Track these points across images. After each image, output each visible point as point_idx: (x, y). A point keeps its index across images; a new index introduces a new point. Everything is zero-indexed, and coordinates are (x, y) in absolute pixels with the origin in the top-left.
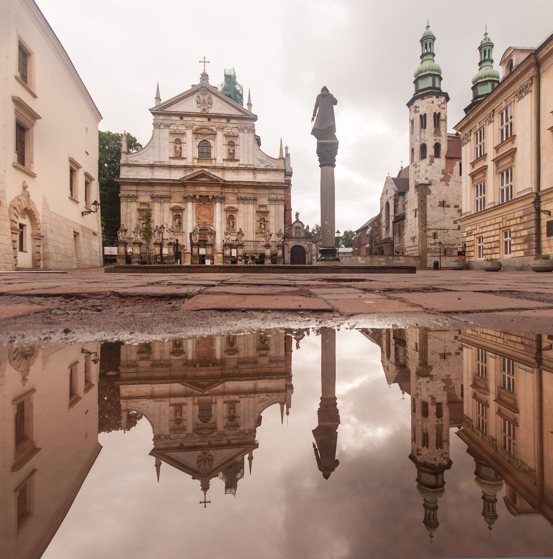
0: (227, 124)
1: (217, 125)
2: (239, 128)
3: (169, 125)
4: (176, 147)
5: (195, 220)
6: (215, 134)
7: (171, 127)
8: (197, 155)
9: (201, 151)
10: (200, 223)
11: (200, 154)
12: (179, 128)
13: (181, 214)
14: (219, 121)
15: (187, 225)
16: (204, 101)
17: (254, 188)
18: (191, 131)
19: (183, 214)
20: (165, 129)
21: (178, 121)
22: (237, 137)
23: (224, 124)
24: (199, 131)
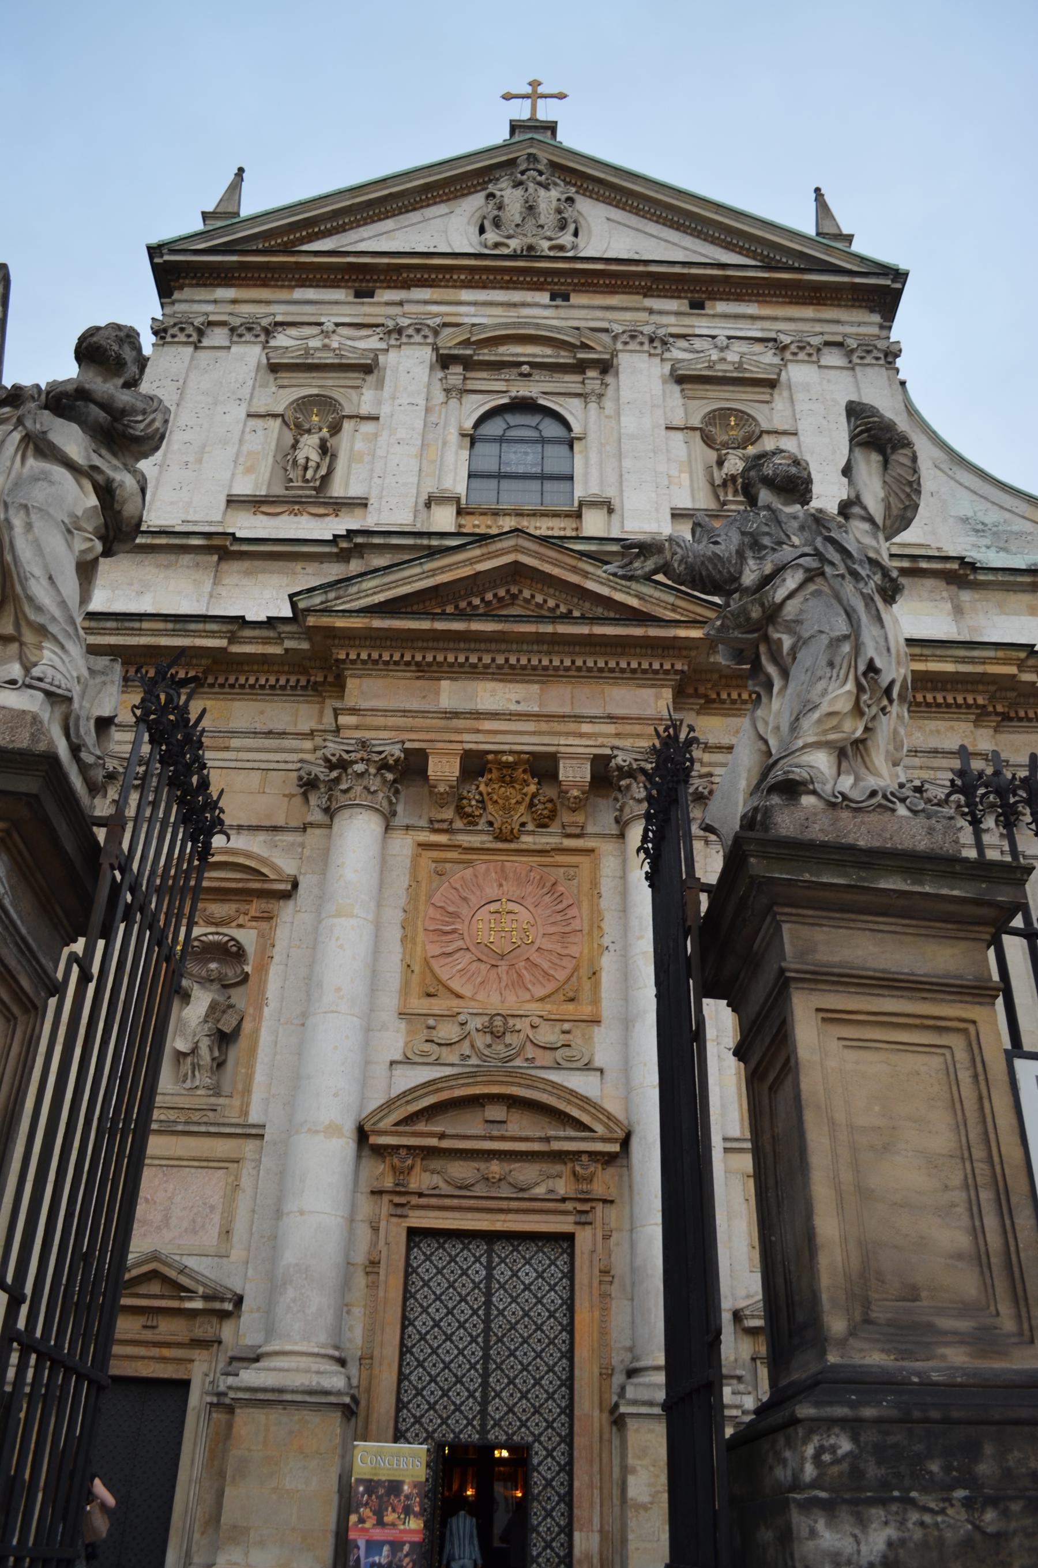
0: (687, 321)
1: (619, 321)
2: (786, 339)
3: (265, 322)
4: (294, 447)
5: (390, 1001)
6: (606, 367)
7: (281, 340)
8: (458, 484)
9: (492, 466)
10: (448, 1031)
11: (477, 483)
12: (335, 345)
13: (247, 937)
14: (638, 305)
15: (300, 1052)
16: (531, 209)
17: (981, 716)
18: (427, 354)
19: (267, 943)
20: (235, 349)
21: (336, 309)
22: (772, 384)
23: (672, 320)
24: (486, 355)
